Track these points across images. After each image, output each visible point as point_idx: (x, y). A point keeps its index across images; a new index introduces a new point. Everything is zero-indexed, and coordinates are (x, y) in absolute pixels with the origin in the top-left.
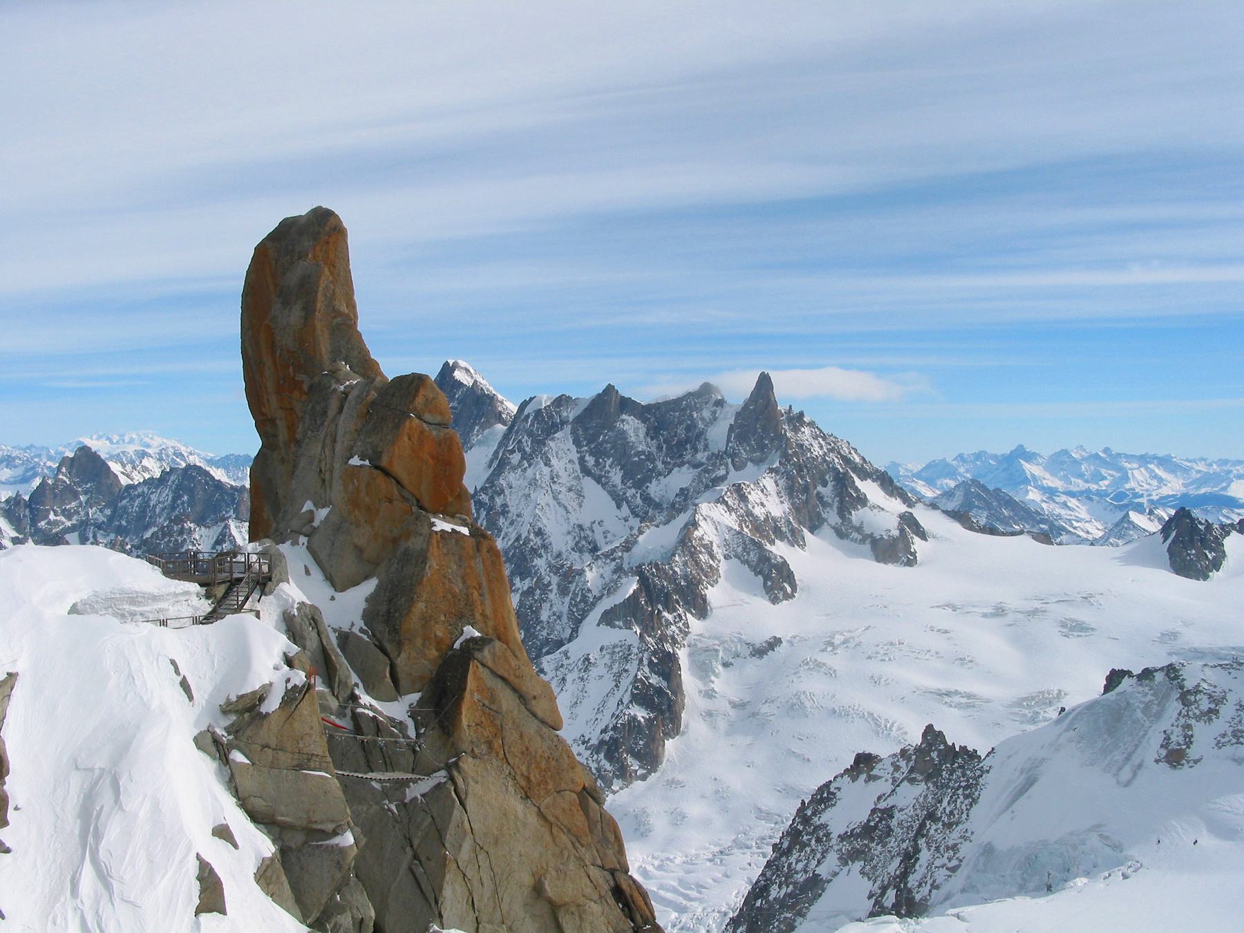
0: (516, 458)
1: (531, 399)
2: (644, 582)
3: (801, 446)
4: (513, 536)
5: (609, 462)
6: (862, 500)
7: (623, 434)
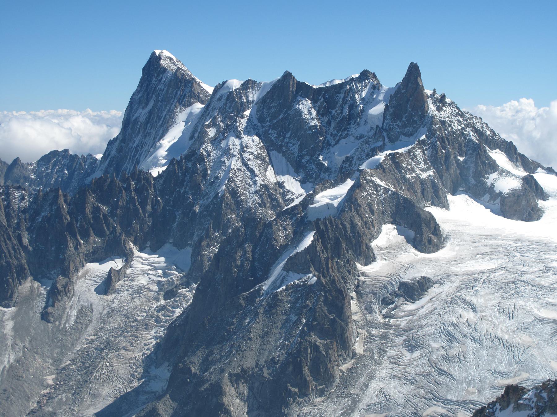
0: (212, 132)
1: (224, 83)
2: (321, 235)
3: (443, 122)
4: (212, 195)
5: (288, 135)
6: (493, 166)
7: (299, 113)
